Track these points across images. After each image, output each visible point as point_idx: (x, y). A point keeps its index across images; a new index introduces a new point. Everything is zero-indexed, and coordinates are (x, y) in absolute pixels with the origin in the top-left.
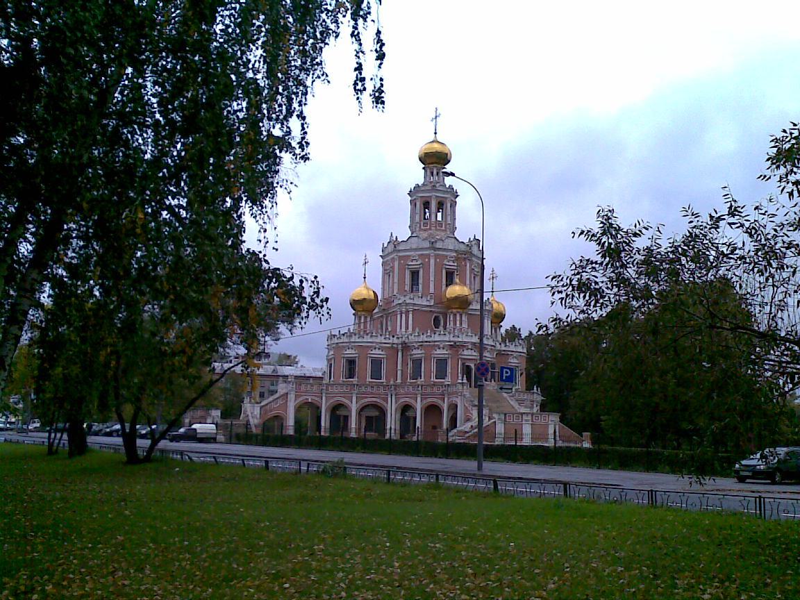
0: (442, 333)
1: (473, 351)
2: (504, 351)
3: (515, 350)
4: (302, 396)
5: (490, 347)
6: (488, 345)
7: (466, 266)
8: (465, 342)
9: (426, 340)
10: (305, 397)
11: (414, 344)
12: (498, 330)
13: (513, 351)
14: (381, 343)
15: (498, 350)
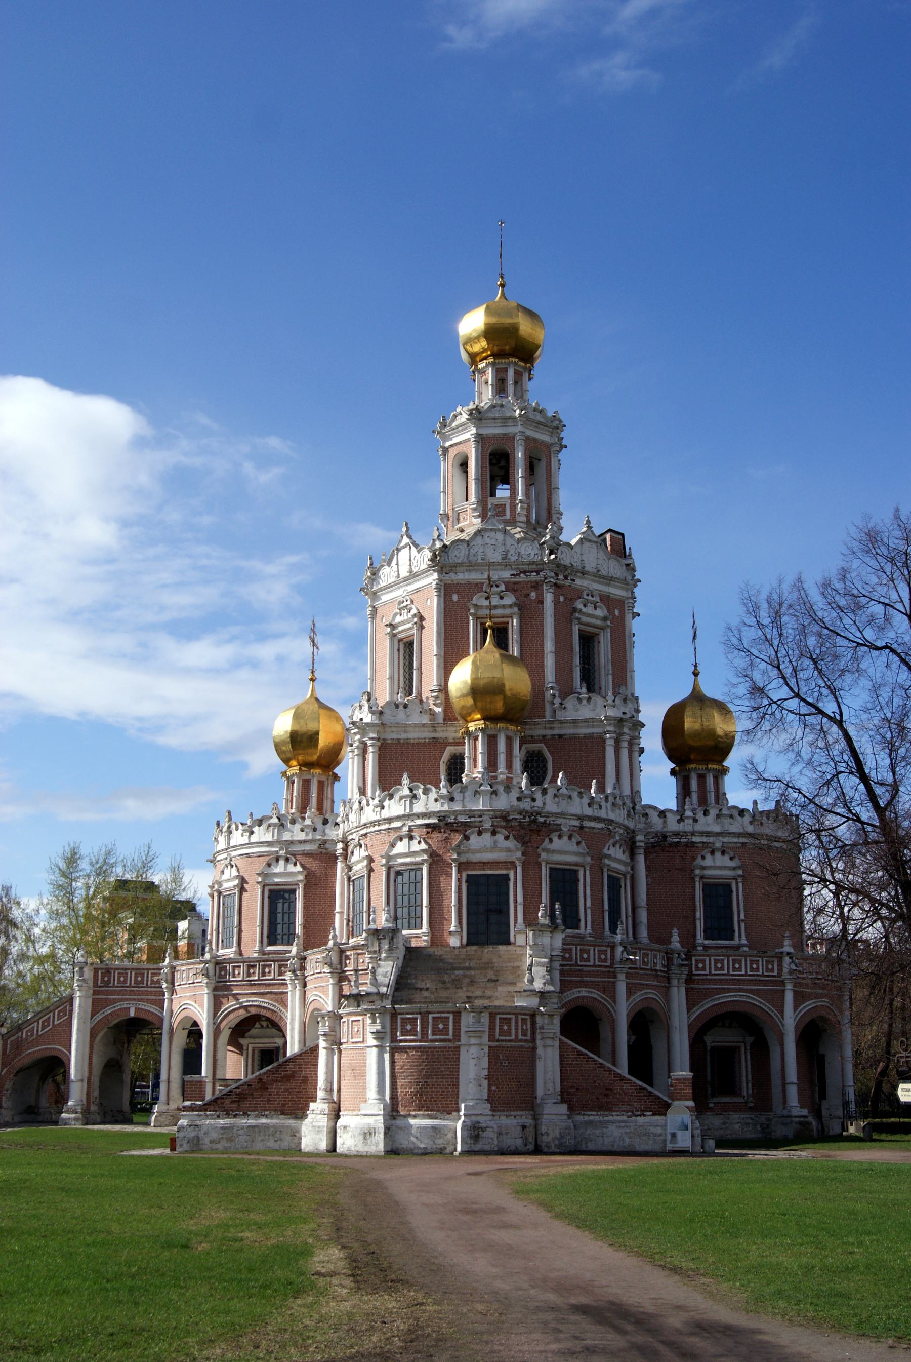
0: (406, 792)
1: (500, 837)
2: (676, 834)
3: (717, 829)
4: (115, 1001)
5: (576, 823)
6: (562, 815)
7: (542, 602)
8: (471, 814)
9: (374, 817)
10: (119, 1006)
11: (354, 836)
12: (710, 780)
13: (708, 834)
14: (292, 842)
15: (656, 835)
